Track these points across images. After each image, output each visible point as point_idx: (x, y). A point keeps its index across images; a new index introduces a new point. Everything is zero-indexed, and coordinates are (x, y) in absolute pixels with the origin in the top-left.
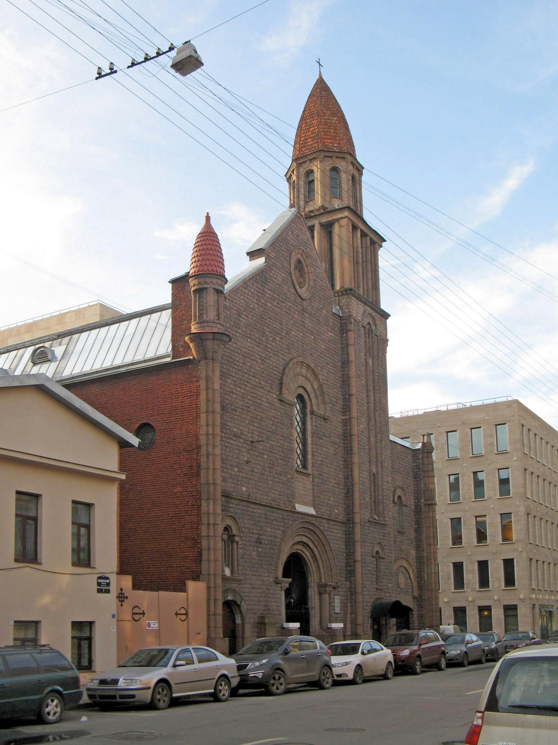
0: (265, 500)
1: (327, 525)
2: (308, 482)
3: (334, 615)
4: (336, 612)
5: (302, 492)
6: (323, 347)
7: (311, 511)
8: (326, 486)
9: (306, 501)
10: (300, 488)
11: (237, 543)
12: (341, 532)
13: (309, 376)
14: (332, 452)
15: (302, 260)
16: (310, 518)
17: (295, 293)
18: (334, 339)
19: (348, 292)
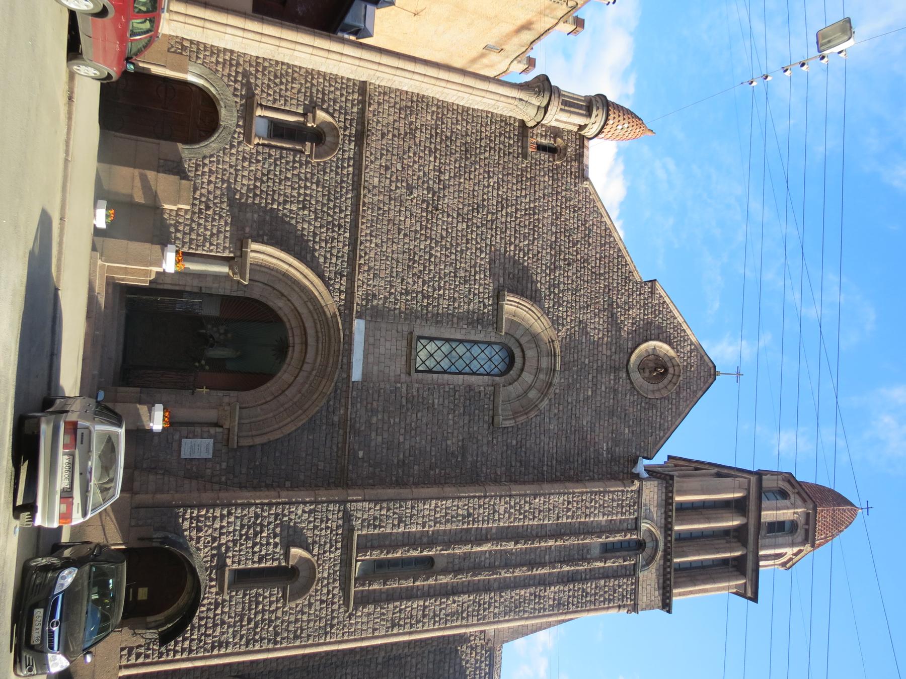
0: (364, 231)
1: (336, 419)
2: (398, 372)
3: (177, 437)
4: (184, 440)
5: (382, 350)
6: (585, 423)
7: (357, 374)
8: (397, 420)
9: (371, 359)
10: (388, 345)
11: (302, 152)
12: (328, 469)
13: (542, 376)
14: (449, 442)
15: (669, 376)
16: (345, 361)
17: (629, 351)
18: (601, 458)
19: (668, 478)
